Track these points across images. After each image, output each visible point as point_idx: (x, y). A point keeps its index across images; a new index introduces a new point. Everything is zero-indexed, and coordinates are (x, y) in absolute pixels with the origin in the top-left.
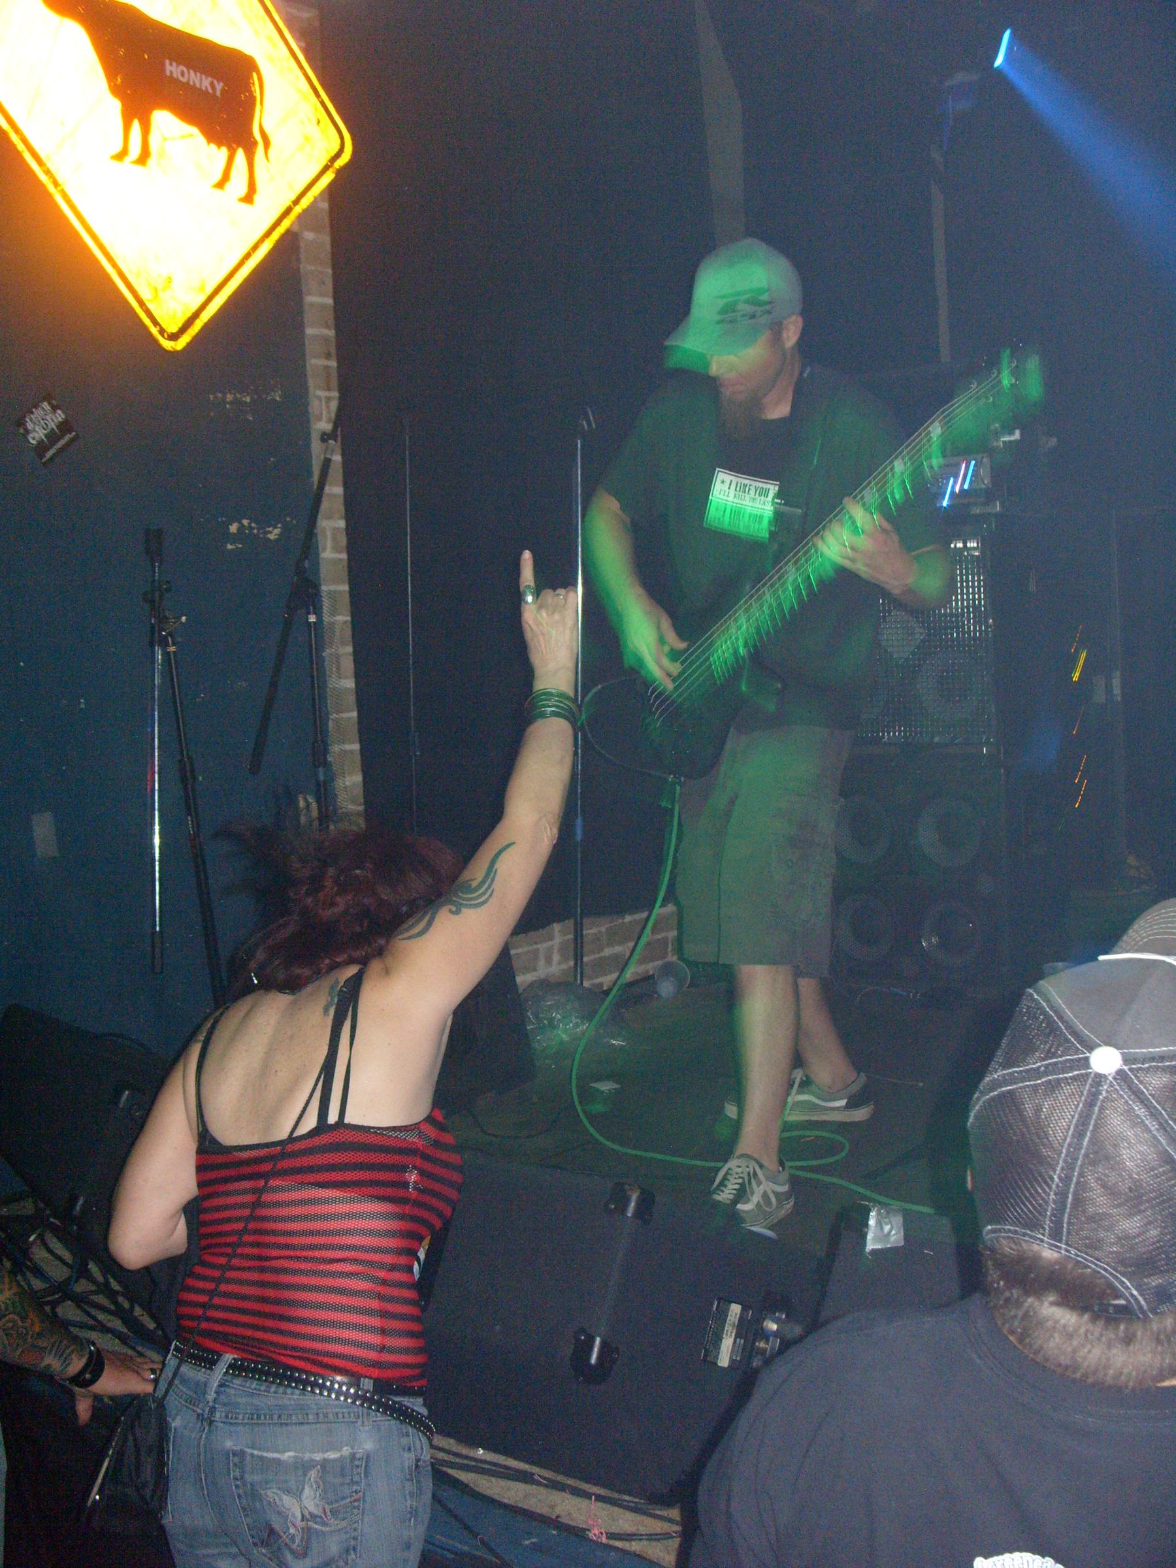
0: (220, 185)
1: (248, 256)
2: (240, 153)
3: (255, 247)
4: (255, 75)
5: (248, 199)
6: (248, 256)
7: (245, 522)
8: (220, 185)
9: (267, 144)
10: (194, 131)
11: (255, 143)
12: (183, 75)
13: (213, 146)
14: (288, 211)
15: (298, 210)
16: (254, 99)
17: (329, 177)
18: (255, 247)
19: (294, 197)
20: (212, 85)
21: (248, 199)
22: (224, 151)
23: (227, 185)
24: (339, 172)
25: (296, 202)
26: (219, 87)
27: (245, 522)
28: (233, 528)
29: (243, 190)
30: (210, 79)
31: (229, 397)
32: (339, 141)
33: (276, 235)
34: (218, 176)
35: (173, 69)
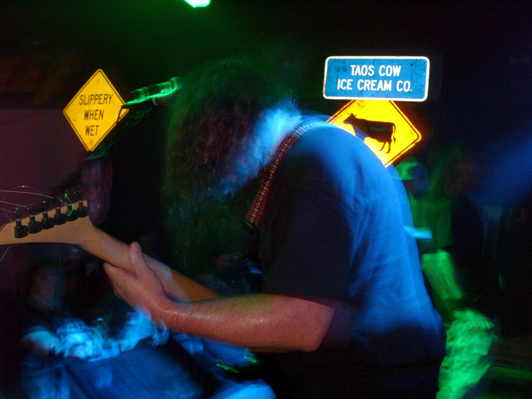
0: (381, 150)
2: (387, 143)
5: (388, 152)
8: (381, 150)
9: (395, 139)
10: (376, 140)
15: (402, 153)
21: (388, 152)
22: (383, 143)
25: (402, 151)
29: (387, 151)
33: (395, 159)
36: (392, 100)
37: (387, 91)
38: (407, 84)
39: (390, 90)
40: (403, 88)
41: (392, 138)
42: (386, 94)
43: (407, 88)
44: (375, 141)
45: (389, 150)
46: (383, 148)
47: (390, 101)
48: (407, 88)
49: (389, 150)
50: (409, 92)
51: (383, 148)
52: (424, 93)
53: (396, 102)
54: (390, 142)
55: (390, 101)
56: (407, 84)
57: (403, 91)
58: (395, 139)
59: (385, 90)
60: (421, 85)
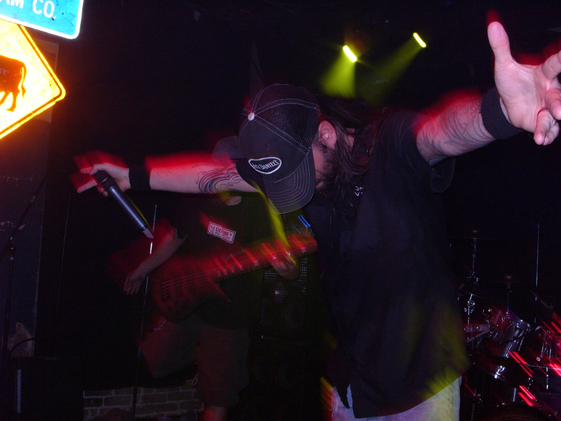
1: (7, 129)
2: (11, 95)
4: (23, 69)
6: (7, 129)
7: (8, 222)
9: (24, 91)
11: (18, 91)
14: (30, 115)
15: (35, 114)
16: (21, 76)
19: (34, 110)
24: (57, 103)
26: (5, 72)
27: (8, 222)
28: (3, 224)
29: (10, 106)
32: (59, 92)
37: (17, 8)
38: (49, 6)
39: (21, 7)
40: (43, 11)
41: (20, 88)
42: (15, 12)
43: (49, 12)
47: (19, 25)
48: (49, 12)
50: (53, 19)
53: (30, 30)
54: (16, 92)
55: (19, 25)
56: (49, 6)
57: (43, 15)
59: (12, 4)
60: (70, 14)
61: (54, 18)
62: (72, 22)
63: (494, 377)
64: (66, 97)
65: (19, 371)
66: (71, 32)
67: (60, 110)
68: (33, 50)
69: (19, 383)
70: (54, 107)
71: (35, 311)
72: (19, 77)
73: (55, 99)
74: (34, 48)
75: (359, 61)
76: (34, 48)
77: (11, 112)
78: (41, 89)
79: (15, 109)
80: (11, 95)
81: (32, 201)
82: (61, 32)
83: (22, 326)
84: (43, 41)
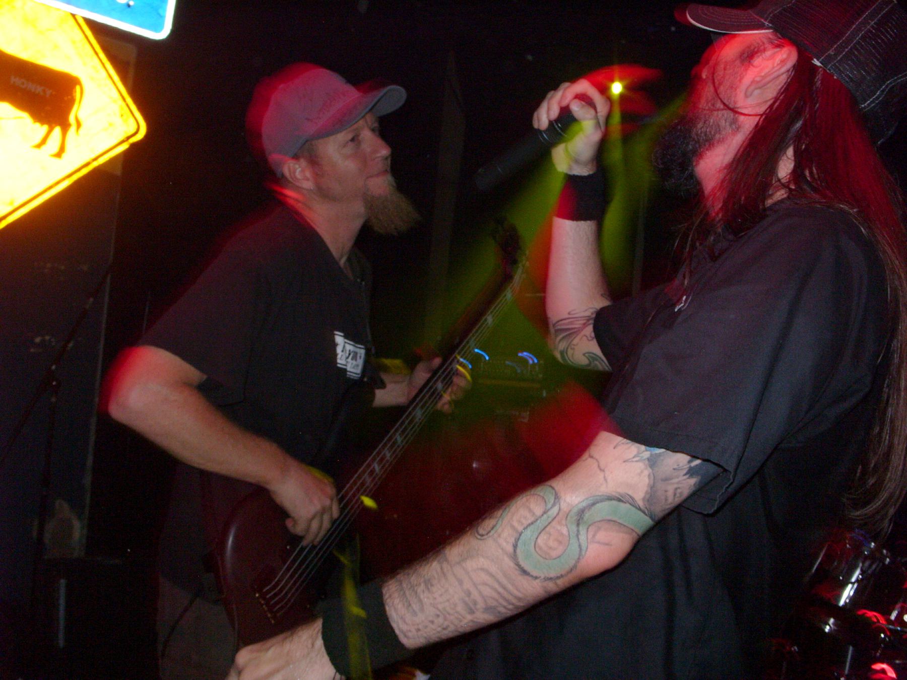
0: (39, 146)
1: (50, 188)
2: (57, 130)
3: (58, 183)
4: (78, 88)
5: (59, 155)
6: (50, 188)
7: (47, 338)
8: (39, 146)
9: (79, 125)
12: (23, 84)
13: (38, 125)
17: (125, 146)
18: (58, 183)
20: (44, 91)
21: (59, 155)
22: (46, 128)
23: (43, 147)
24: (133, 146)
26: (49, 92)
28: (38, 340)
29: (56, 150)
30: (42, 88)
31: (49, 265)
32: (136, 127)
34: (39, 141)
35: (16, 80)
36: (84, 13)
41: (72, 119)
44: (24, 118)
45: (62, 149)
46: (44, 141)
47: (74, 16)
49: (62, 149)
50: (129, 6)
51: (44, 141)
52: (161, 17)
53: (92, 24)
54: (65, 126)
55: (74, 16)
58: (79, 125)
61: (131, 3)
62: (161, 11)
63: (823, 631)
64: (146, 136)
65: (63, 582)
66: (158, 28)
67: (135, 155)
68: (95, 57)
69: (62, 602)
70: (126, 153)
71: (88, 480)
72: (72, 101)
73: (128, 138)
74: (97, 53)
75: (626, 82)
76: (97, 53)
77: (57, 159)
78: (108, 122)
79: (63, 155)
80: (57, 130)
81: (87, 307)
82: (140, 26)
83: (66, 506)
84: (110, 40)
